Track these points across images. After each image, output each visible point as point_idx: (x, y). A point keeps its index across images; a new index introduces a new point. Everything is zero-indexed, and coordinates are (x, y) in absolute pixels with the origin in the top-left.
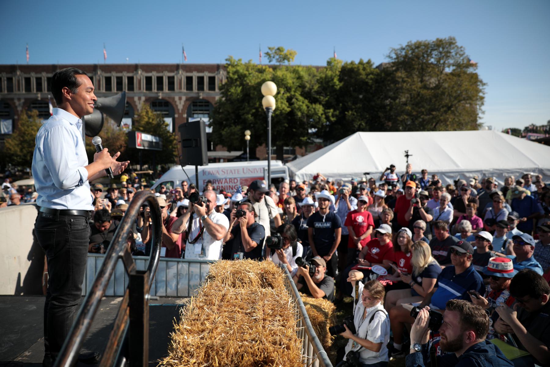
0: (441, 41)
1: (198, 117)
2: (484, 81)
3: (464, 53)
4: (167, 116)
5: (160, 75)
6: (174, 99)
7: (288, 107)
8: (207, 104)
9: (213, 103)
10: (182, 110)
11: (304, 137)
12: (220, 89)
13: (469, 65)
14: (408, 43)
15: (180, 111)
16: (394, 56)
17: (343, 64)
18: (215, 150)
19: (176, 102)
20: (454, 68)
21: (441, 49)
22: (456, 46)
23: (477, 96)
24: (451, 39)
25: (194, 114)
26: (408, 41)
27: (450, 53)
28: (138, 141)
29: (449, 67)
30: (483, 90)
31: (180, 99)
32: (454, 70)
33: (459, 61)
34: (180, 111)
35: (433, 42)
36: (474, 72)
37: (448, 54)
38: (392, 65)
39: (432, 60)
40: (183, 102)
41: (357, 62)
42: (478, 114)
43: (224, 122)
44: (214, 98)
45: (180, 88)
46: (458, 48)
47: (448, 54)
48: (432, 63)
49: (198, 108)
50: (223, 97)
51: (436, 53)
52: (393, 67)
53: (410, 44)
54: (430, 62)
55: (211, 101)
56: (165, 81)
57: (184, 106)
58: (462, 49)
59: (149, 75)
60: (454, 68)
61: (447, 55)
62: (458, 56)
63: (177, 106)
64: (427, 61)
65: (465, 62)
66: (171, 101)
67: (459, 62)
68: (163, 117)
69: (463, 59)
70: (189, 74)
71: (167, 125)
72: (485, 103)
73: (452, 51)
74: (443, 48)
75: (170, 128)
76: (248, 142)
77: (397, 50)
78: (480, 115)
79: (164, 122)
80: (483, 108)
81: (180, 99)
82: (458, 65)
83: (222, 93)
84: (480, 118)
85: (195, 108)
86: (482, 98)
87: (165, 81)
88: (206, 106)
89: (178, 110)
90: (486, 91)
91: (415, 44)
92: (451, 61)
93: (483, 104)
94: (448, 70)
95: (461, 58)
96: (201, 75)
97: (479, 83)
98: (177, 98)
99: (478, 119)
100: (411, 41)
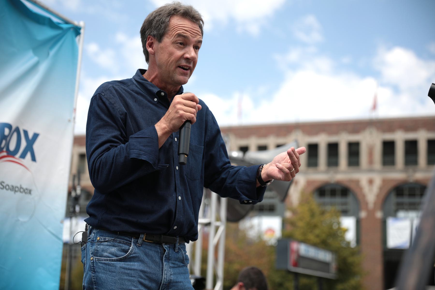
1: (405, 218)
4: (345, 213)
5: (333, 139)
6: (357, 182)
10: (375, 204)
15: (371, 205)
19: (361, 189)
25: (396, 211)
28: (293, 258)
31: (371, 182)
34: (371, 205)
40: (375, 188)
45: (371, 161)
49: (406, 200)
56: (343, 150)
57: (378, 196)
59: (314, 140)
63: (364, 196)
66: (352, 186)
68: (338, 217)
70: (388, 137)
71: (346, 231)
75: (351, 236)
79: (339, 223)
81: (371, 182)
85: (401, 200)
87: (343, 150)
89: (367, 204)
96: (411, 136)
98: (364, 182)
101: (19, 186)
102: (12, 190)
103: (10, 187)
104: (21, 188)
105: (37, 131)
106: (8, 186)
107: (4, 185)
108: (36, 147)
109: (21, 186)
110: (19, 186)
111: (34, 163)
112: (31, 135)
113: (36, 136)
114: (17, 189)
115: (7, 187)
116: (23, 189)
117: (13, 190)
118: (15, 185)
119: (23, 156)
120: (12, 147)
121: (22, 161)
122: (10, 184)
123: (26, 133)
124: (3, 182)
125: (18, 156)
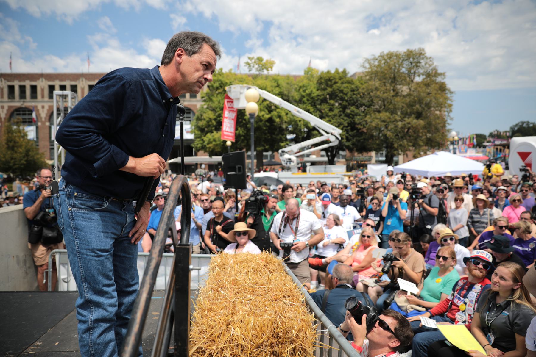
0: (411, 52)
2: (452, 90)
3: (433, 63)
7: (267, 114)
8: (188, 111)
9: (195, 111)
11: (283, 142)
12: (202, 98)
13: (437, 74)
14: (381, 53)
16: (367, 65)
17: (319, 73)
18: (196, 155)
20: (424, 77)
21: (411, 60)
22: (426, 57)
23: (446, 103)
24: (421, 50)
26: (381, 51)
27: (420, 63)
29: (419, 76)
30: (451, 98)
32: (424, 79)
33: (428, 71)
35: (405, 53)
36: (443, 81)
37: (418, 64)
38: (366, 74)
39: (404, 70)
41: (333, 71)
42: (447, 121)
43: (206, 129)
44: (196, 106)
46: (427, 58)
47: (418, 64)
48: (403, 73)
50: (205, 105)
51: (407, 63)
52: (366, 76)
53: (382, 54)
54: (401, 71)
55: (192, 108)
58: (431, 59)
60: (424, 77)
61: (417, 65)
62: (427, 66)
64: (399, 70)
65: (434, 72)
67: (428, 72)
69: (432, 69)
72: (453, 110)
73: (422, 61)
74: (414, 59)
76: (229, 148)
77: (371, 60)
78: (449, 121)
80: (451, 115)
82: (428, 75)
83: (205, 101)
84: (448, 124)
86: (450, 106)
88: (187, 113)
90: (454, 98)
91: (387, 55)
92: (421, 71)
93: (451, 111)
94: (418, 79)
95: (431, 68)
97: (447, 92)
99: (447, 125)
100: (383, 52)
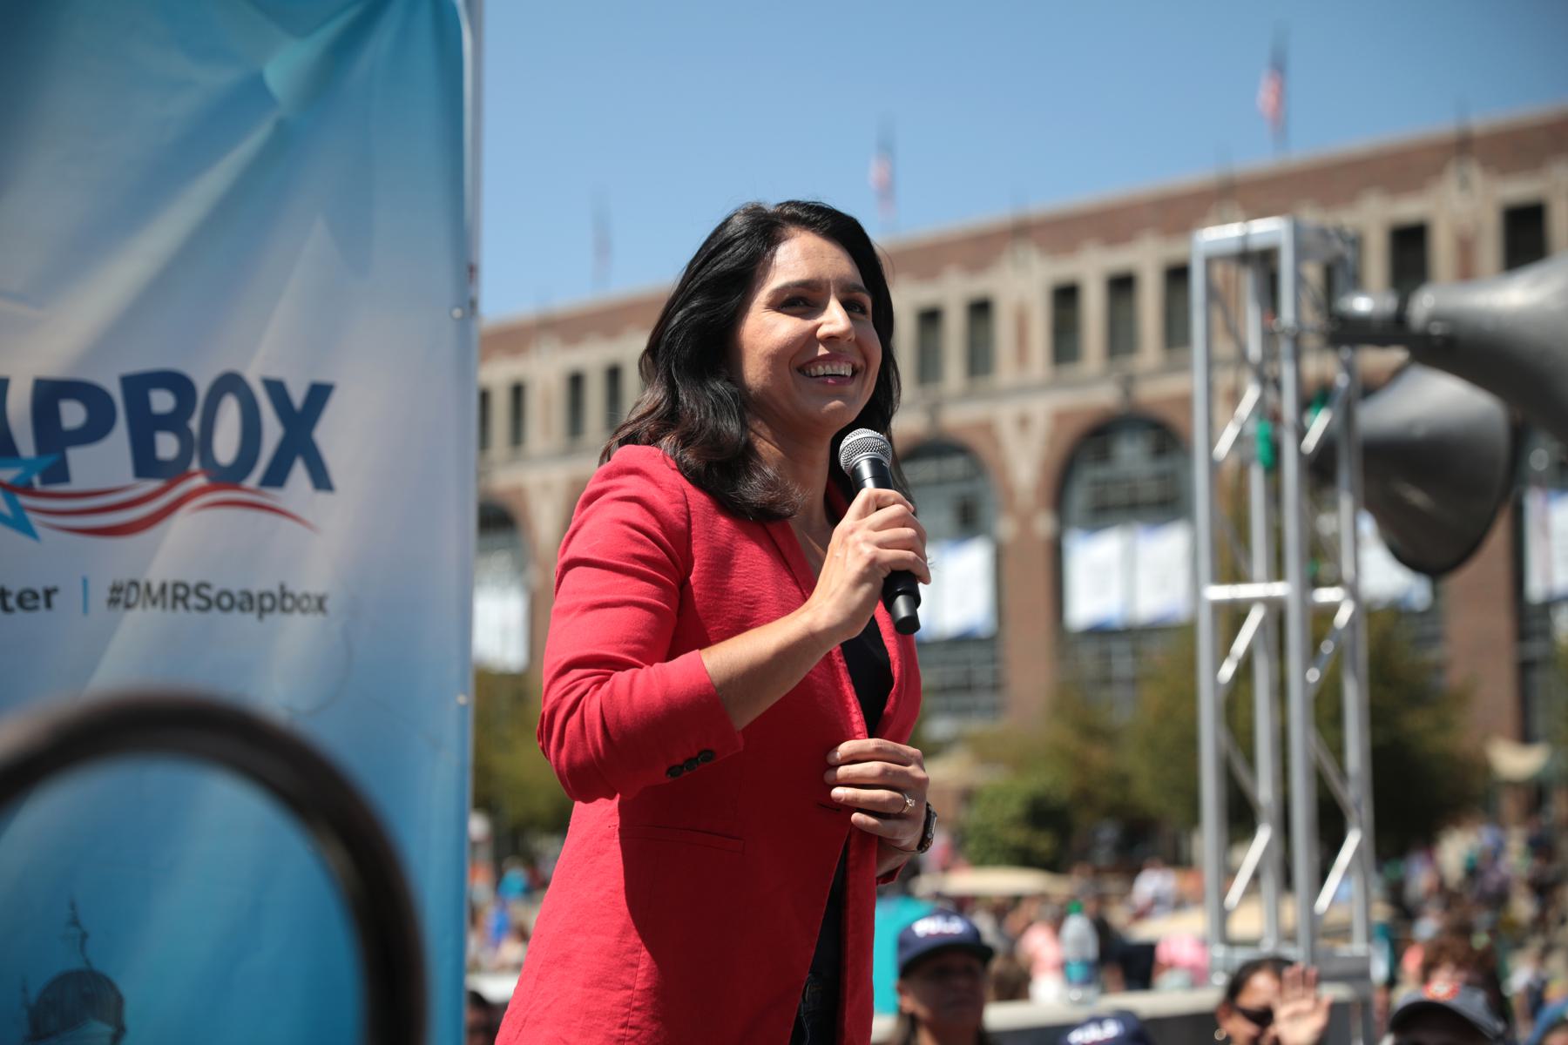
101: (276, 591)
102: (247, 605)
103: (238, 598)
104: (284, 595)
105: (322, 377)
106: (230, 595)
107: (212, 594)
108: (329, 435)
109: (282, 587)
110: (276, 591)
111: (322, 497)
112: (298, 396)
113: (319, 394)
114: (267, 602)
115: (226, 601)
116: (292, 596)
117: (251, 609)
118: (255, 590)
119: (276, 476)
120: (226, 445)
121: (274, 496)
122: (235, 587)
123: (276, 389)
124: (207, 586)
125: (253, 480)
